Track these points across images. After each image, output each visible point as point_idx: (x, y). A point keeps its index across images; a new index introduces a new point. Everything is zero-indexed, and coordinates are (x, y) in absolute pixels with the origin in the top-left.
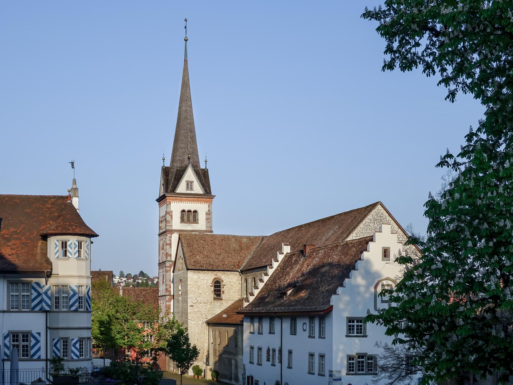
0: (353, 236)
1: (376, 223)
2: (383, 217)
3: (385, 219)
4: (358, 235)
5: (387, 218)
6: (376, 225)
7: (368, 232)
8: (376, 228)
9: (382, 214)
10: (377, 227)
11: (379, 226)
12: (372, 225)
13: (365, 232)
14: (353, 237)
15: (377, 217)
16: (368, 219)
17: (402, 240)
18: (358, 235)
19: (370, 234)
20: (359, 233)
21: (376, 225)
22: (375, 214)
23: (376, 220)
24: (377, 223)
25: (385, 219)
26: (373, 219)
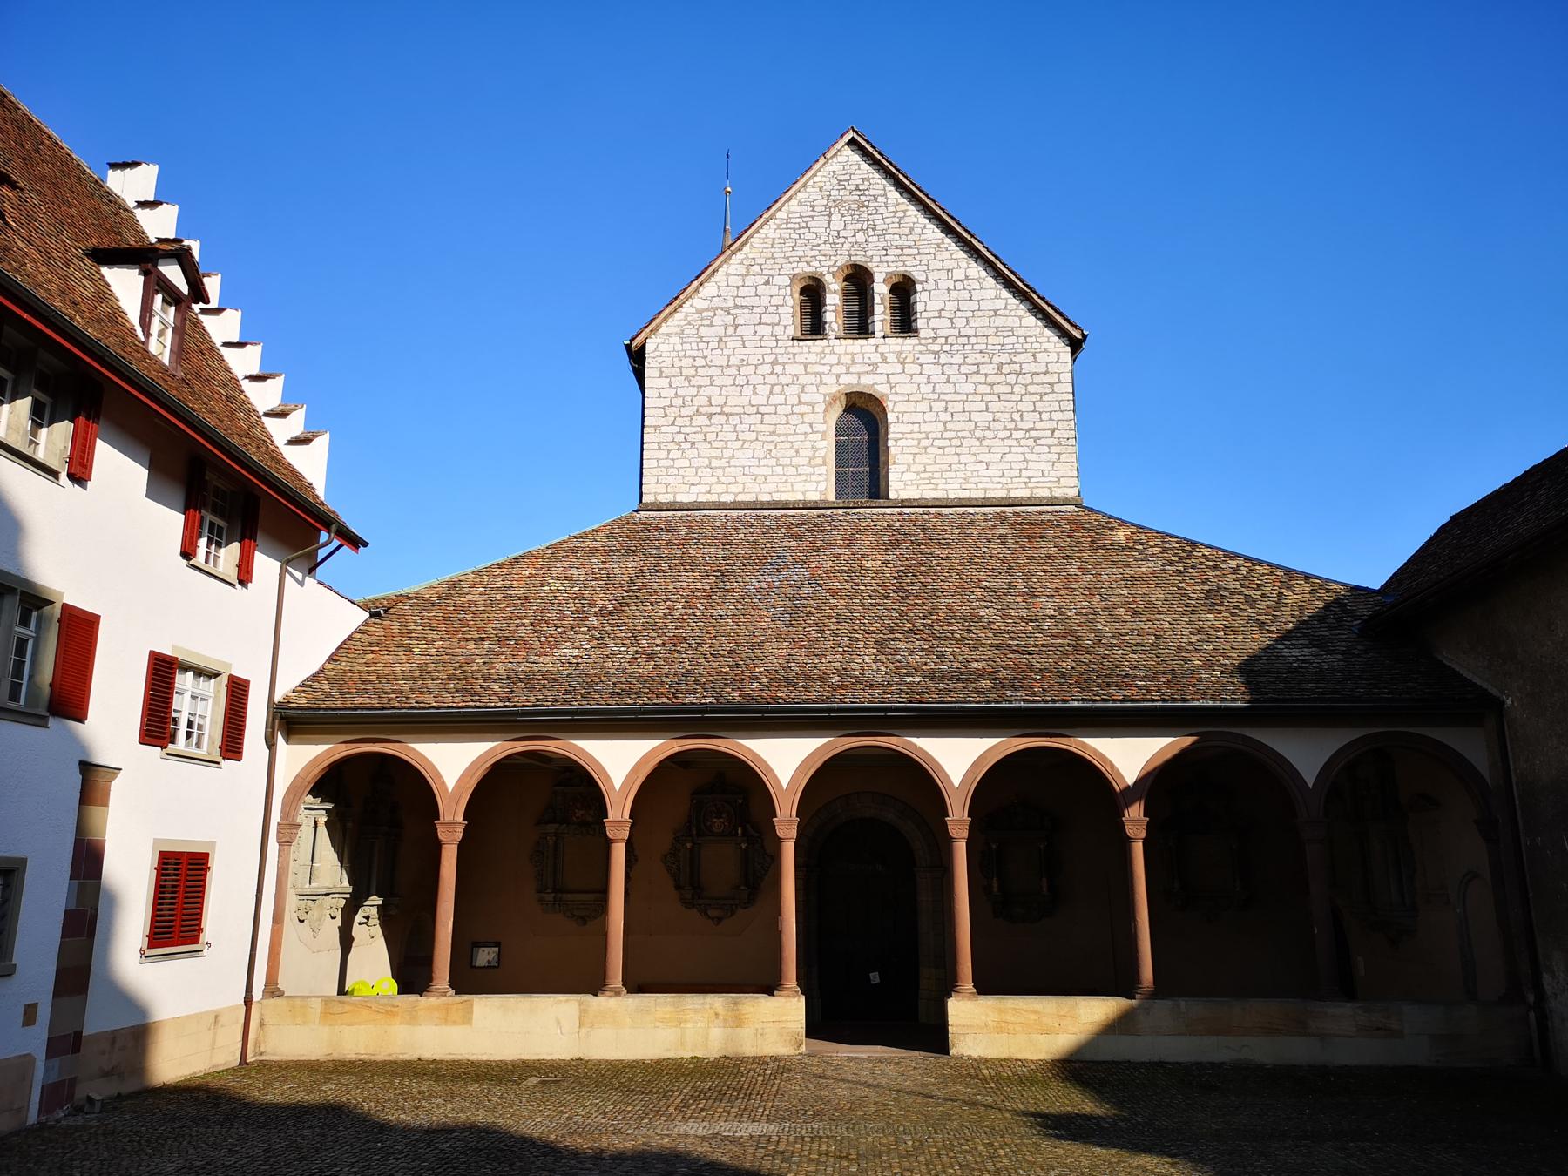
0: (728, 275)
1: (835, 217)
2: (871, 192)
3: (881, 199)
4: (756, 268)
5: (889, 195)
6: (837, 225)
7: (802, 254)
8: (838, 237)
9: (864, 179)
10: (842, 234)
11: (850, 227)
12: (818, 225)
13: (788, 254)
14: (731, 278)
15: (842, 193)
16: (800, 204)
17: (967, 278)
18: (756, 268)
19: (808, 264)
20: (758, 261)
21: (837, 225)
22: (835, 182)
23: (838, 204)
24: (842, 215)
25: (881, 199)
26: (825, 202)
